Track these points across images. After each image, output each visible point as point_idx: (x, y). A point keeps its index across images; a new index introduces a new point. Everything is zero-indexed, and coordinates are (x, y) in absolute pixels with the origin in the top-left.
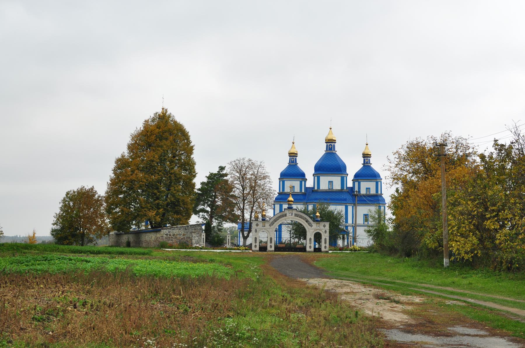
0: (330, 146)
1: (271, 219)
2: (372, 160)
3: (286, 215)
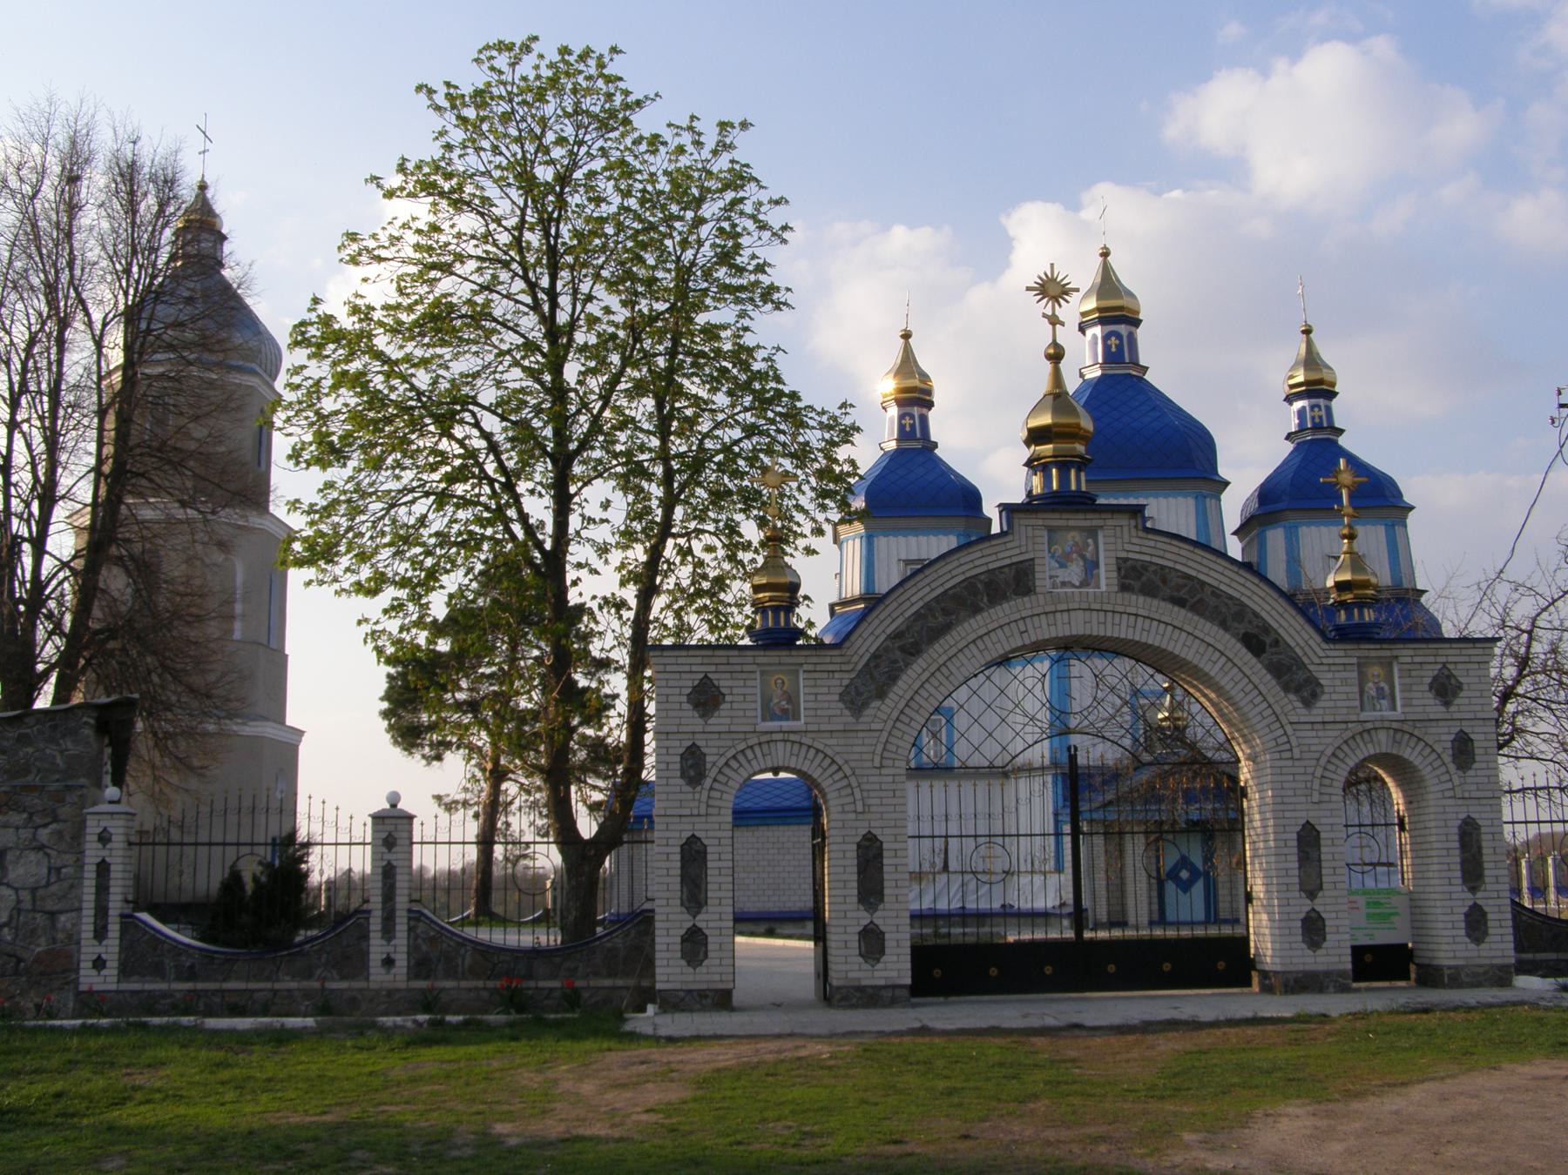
0: (1113, 341)
1: (882, 613)
2: (1342, 410)
3: (1020, 580)
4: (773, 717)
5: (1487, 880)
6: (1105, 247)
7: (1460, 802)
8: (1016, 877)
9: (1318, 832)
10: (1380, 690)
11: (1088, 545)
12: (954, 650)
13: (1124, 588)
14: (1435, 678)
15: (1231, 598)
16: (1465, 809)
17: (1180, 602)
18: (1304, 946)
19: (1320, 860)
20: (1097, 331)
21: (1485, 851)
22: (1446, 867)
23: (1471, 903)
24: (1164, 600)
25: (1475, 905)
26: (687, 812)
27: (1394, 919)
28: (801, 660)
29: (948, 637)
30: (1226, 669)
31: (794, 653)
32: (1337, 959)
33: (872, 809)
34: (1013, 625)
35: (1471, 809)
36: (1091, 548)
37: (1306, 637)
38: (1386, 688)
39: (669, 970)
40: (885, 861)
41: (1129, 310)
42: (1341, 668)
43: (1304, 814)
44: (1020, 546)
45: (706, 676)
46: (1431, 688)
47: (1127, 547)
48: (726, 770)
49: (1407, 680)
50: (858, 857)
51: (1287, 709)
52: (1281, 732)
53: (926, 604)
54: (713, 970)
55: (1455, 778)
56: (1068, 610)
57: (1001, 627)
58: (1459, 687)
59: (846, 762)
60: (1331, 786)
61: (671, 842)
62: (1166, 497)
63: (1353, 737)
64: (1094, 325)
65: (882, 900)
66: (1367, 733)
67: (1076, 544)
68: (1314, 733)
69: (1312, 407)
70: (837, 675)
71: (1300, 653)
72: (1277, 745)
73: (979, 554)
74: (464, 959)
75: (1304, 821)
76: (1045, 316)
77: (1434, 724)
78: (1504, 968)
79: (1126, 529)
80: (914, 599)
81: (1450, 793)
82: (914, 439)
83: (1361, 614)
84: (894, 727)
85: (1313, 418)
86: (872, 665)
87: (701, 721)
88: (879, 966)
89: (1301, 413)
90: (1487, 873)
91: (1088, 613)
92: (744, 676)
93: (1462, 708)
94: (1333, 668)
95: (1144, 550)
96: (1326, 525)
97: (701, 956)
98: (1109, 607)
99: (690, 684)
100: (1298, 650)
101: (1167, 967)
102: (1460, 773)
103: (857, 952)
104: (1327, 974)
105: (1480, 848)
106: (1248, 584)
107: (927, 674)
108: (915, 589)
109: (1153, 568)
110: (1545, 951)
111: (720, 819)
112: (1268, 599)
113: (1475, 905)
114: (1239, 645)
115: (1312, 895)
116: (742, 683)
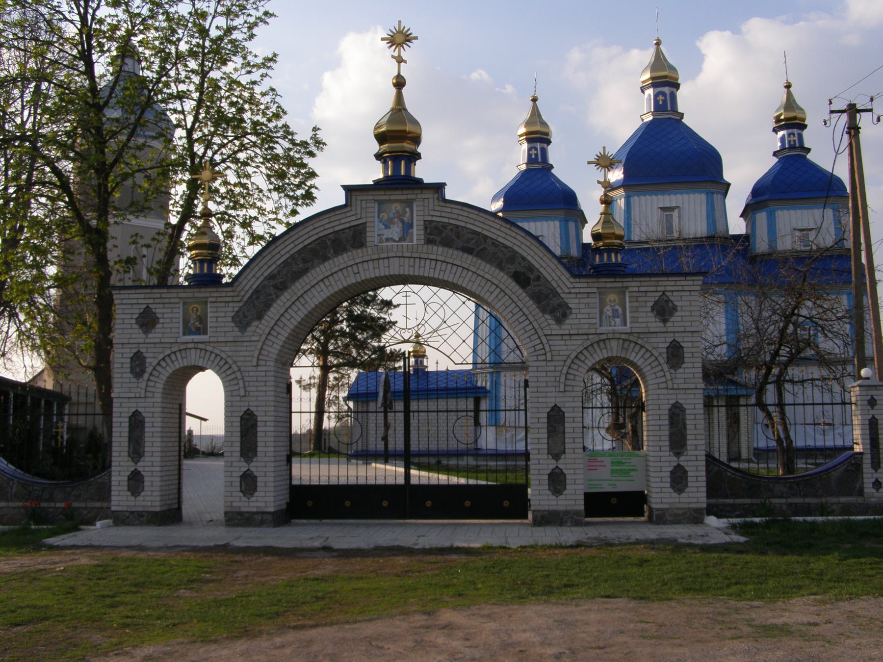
0: (661, 98)
4: (191, 333)
5: (689, 448)
6: (658, 39)
7: (671, 392)
8: (590, 431)
9: (564, 413)
10: (615, 312)
11: (406, 213)
12: (309, 286)
13: (429, 241)
14: (656, 303)
15: (506, 247)
16: (675, 397)
17: (468, 251)
18: (549, 493)
19: (564, 433)
20: (650, 92)
21: (688, 427)
22: (658, 438)
23: (675, 464)
24: (457, 249)
25: (679, 465)
26: (133, 395)
27: (632, 473)
28: (208, 295)
29: (305, 278)
30: (499, 297)
31: (221, 289)
32: (573, 502)
33: (251, 394)
34: (349, 269)
35: (679, 396)
36: (408, 215)
37: (559, 274)
38: (620, 309)
39: (120, 498)
40: (259, 429)
41: (671, 78)
42: (586, 295)
43: (553, 400)
44: (356, 214)
45: (148, 307)
46: (653, 309)
47: (432, 213)
48: (158, 368)
49: (635, 304)
50: (241, 426)
51: (543, 325)
52: (538, 341)
53: (292, 255)
54: (147, 498)
55: (668, 374)
56: (388, 258)
57: (341, 270)
58: (675, 309)
59: (235, 362)
60: (574, 380)
61: (123, 415)
62: (688, 193)
63: (592, 345)
64: (649, 88)
65: (256, 455)
66: (603, 341)
67: (397, 212)
68: (563, 342)
69: (789, 135)
70: (231, 304)
71: (555, 285)
72: (535, 351)
73: (327, 221)
74: (12, 488)
75: (553, 405)
76: (393, 57)
77: (654, 335)
78: (698, 511)
79: (431, 201)
80: (282, 253)
81: (664, 385)
82: (538, 163)
83: (609, 257)
84: (266, 338)
85: (789, 142)
86: (254, 297)
87: (144, 336)
88: (253, 499)
89: (782, 139)
90: (689, 442)
91: (402, 259)
92: (172, 306)
93: (675, 324)
94: (579, 296)
95: (444, 214)
96: (794, 209)
97: (141, 489)
98: (417, 255)
99: (137, 311)
100: (553, 283)
101: (468, 504)
102: (672, 371)
103: (239, 489)
104: (566, 512)
105: (685, 425)
106: (518, 237)
107: (289, 303)
108: (283, 246)
109: (449, 228)
110: (742, 497)
111: (154, 400)
112: (532, 247)
113: (679, 465)
114: (510, 280)
115: (557, 457)
116: (170, 310)
